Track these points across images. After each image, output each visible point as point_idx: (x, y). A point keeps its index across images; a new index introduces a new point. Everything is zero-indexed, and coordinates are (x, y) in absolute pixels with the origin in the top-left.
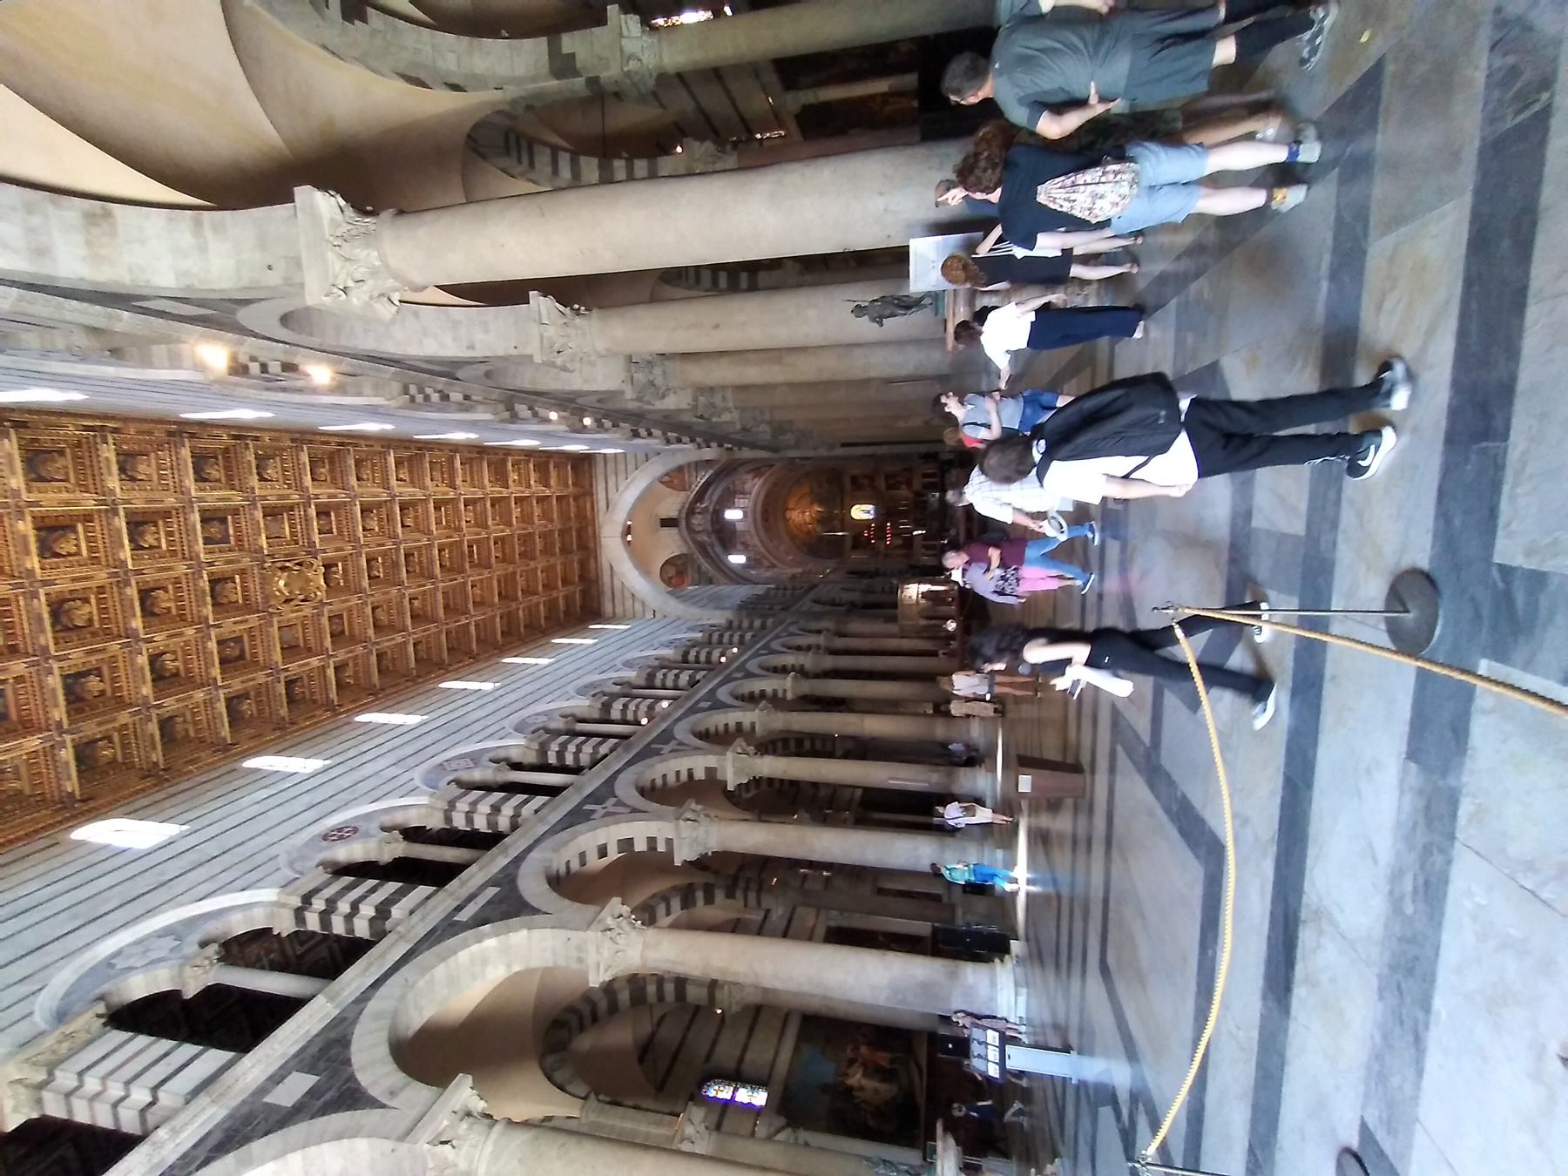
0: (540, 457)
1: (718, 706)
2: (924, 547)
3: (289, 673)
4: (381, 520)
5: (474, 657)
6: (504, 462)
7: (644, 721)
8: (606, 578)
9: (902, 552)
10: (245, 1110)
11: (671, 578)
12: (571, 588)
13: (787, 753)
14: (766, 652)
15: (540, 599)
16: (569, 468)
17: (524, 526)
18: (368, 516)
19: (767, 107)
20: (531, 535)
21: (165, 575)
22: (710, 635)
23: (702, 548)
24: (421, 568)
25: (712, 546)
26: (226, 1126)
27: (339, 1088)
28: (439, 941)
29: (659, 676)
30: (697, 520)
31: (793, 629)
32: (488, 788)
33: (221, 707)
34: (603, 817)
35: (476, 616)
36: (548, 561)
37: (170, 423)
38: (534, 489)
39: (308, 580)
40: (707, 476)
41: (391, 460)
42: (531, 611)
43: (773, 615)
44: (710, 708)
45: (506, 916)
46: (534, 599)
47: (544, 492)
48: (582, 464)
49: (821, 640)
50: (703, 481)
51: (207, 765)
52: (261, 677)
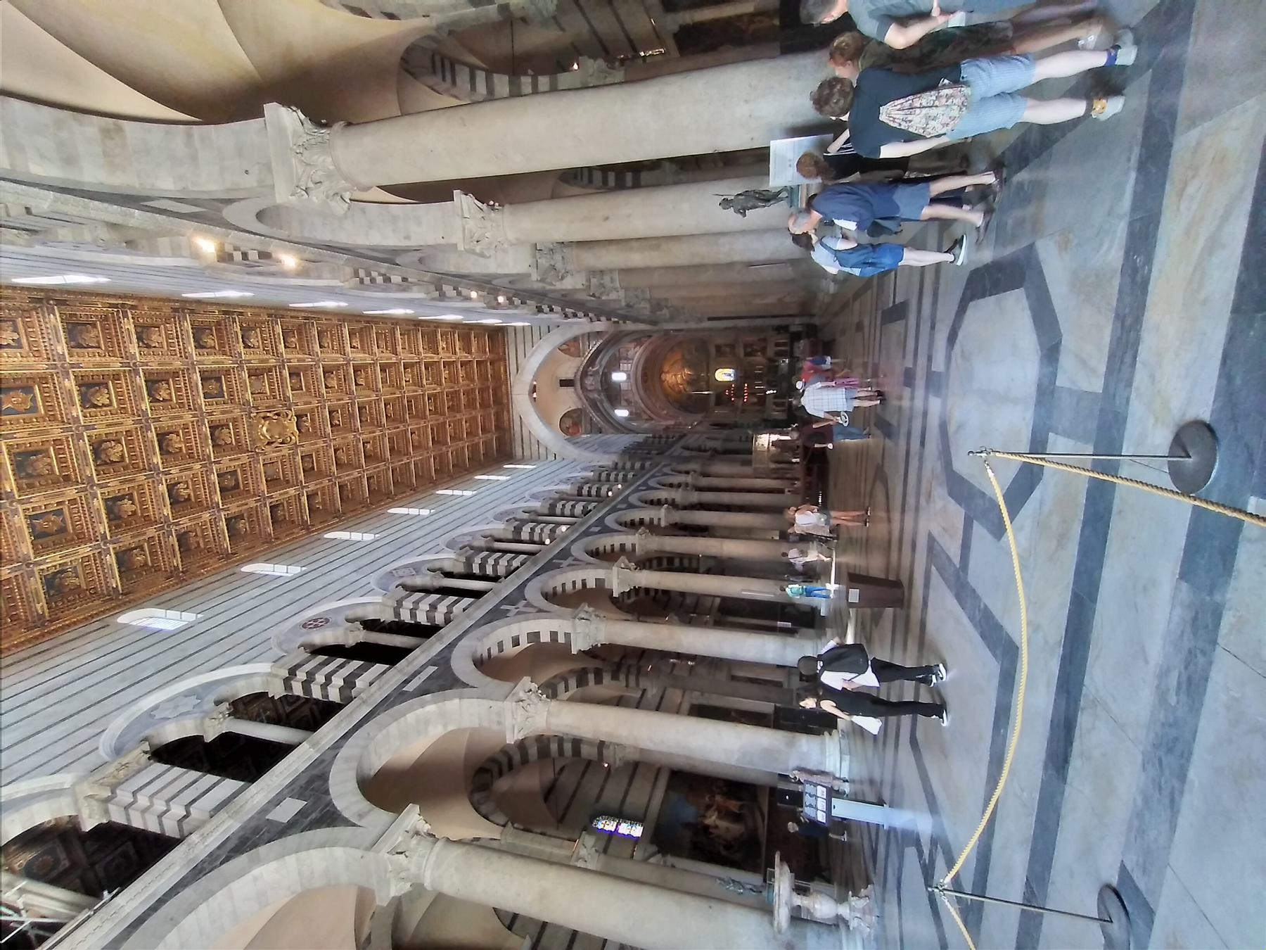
0: (464, 329)
1: (606, 530)
5: (414, 490)
6: (435, 333)
7: (547, 542)
8: (517, 428)
9: (758, 408)
10: (253, 824)
11: (568, 428)
12: (489, 435)
13: (660, 568)
14: (644, 488)
17: (452, 385)
18: (329, 377)
19: (649, 26)
20: (457, 392)
21: (176, 422)
22: (600, 474)
23: (594, 404)
24: (371, 419)
25: (601, 402)
26: (241, 834)
27: (322, 810)
28: (392, 705)
29: (559, 506)
30: (589, 381)
31: (666, 470)
32: (427, 591)
33: (223, 524)
35: (414, 458)
36: (471, 414)
37: (175, 301)
39: (285, 427)
41: (346, 332)
42: (458, 454)
43: (650, 459)
44: (600, 532)
45: (443, 688)
46: (460, 444)
47: (466, 357)
48: (497, 335)
49: (689, 479)
51: (214, 569)
52: (252, 503)
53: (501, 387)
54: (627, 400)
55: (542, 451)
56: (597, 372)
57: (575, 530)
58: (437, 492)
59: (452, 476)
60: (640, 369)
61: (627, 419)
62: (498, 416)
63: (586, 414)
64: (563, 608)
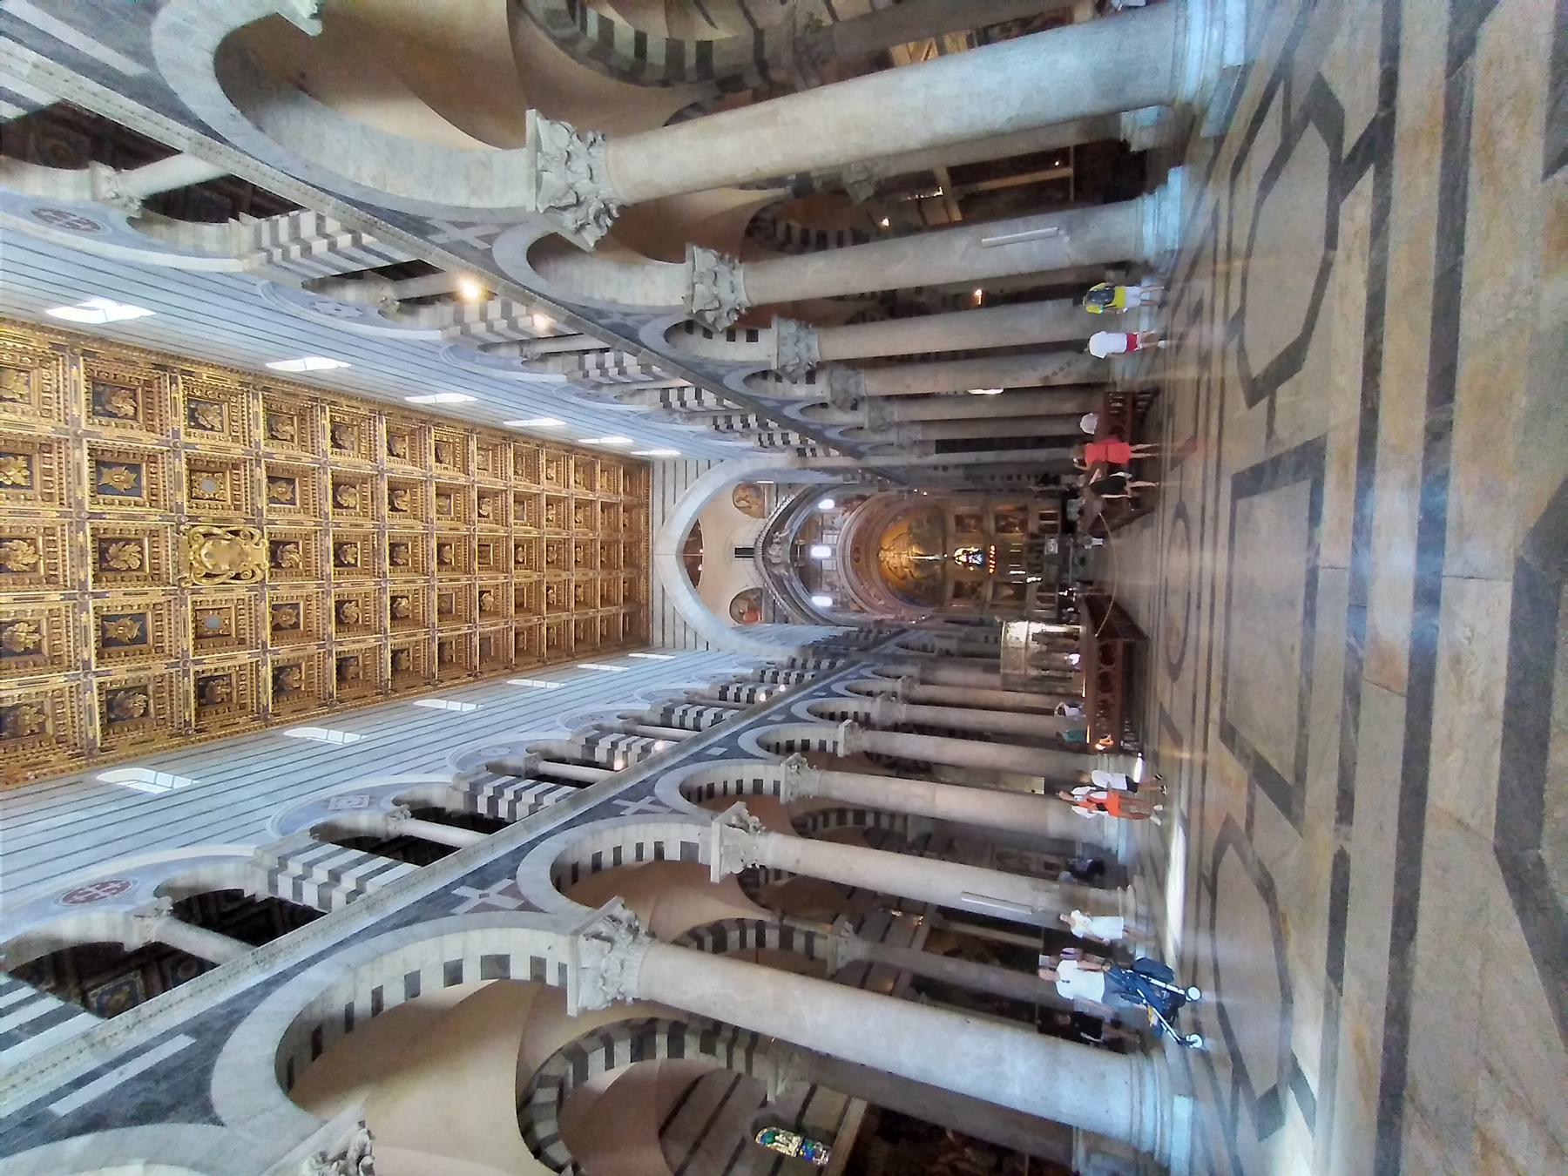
1: (734, 752)
2: (1039, 598)
4: (364, 498)
5: (475, 675)
7: (619, 764)
8: (657, 604)
9: (1016, 603)
11: (742, 614)
12: (613, 609)
14: (824, 694)
17: (557, 530)
18: (346, 491)
23: (779, 582)
25: (790, 580)
29: (678, 711)
30: (774, 551)
31: (867, 672)
38: (573, 490)
39: (243, 554)
40: (788, 502)
41: (382, 429)
43: (845, 656)
44: (722, 757)
48: (636, 470)
49: (898, 686)
50: (783, 508)
52: (159, 667)
53: (640, 541)
55: (690, 637)
56: (786, 538)
57: (681, 750)
58: (509, 682)
59: (544, 662)
60: (849, 542)
61: (832, 610)
62: (631, 584)
63: (768, 596)
64: (574, 906)
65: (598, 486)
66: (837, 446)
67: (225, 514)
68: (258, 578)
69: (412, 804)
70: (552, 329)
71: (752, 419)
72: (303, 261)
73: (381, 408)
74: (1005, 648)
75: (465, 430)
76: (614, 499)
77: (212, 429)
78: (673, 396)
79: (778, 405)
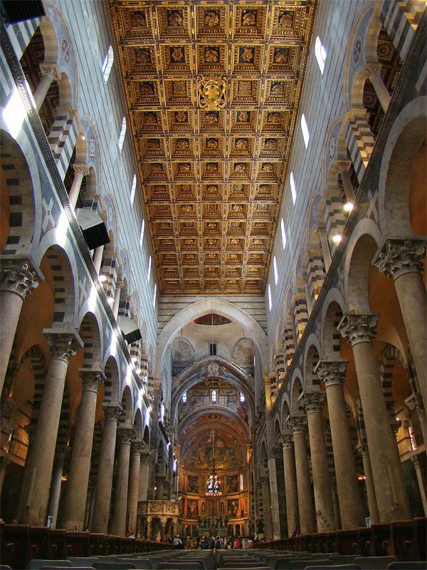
2: (189, 526)
3: (159, 84)
4: (241, 151)
6: (266, 234)
13: (65, 397)
15: (178, 252)
16: (258, 279)
18: (244, 143)
22: (146, 361)
25: (198, 377)
34: (43, 207)
35: (174, 209)
38: (248, 253)
41: (276, 160)
46: (178, 248)
48: (259, 287)
53: (219, 288)
54: (195, 401)
55: (166, 318)
59: (153, 238)
62: (197, 285)
65: (251, 266)
66: (278, 400)
67: (232, 94)
68: (201, 106)
69: (89, 176)
70: (333, 244)
71: (292, 351)
72: (353, 137)
73: (286, 160)
74: (163, 503)
75: (277, 199)
76: (243, 275)
77: (271, 90)
78: (301, 307)
79: (301, 363)
